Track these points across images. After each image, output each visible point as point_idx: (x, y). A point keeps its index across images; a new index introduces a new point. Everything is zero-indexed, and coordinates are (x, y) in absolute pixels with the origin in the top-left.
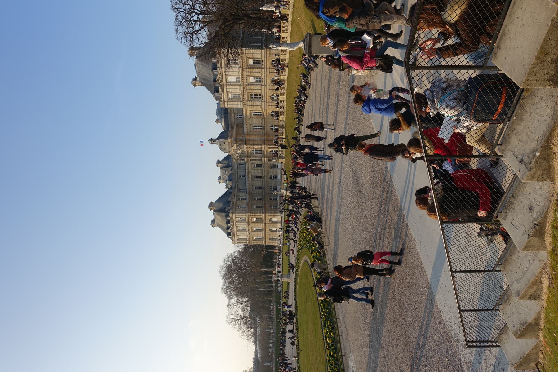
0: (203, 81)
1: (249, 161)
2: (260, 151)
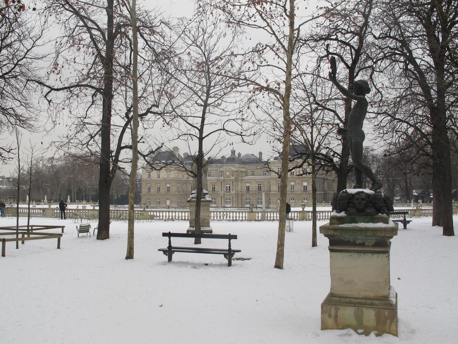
1: (220, 181)
2: (229, 189)
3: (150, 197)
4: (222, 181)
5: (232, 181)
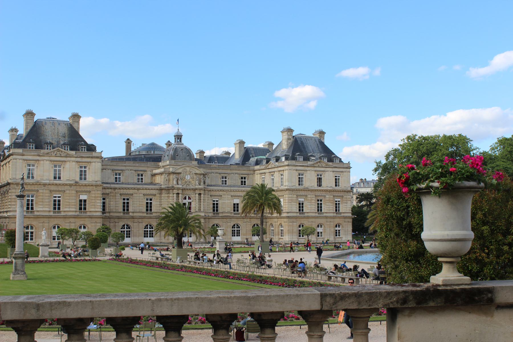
0: (299, 142)
1: (175, 191)
3: (34, 223)
4: (180, 192)
5: (198, 192)
